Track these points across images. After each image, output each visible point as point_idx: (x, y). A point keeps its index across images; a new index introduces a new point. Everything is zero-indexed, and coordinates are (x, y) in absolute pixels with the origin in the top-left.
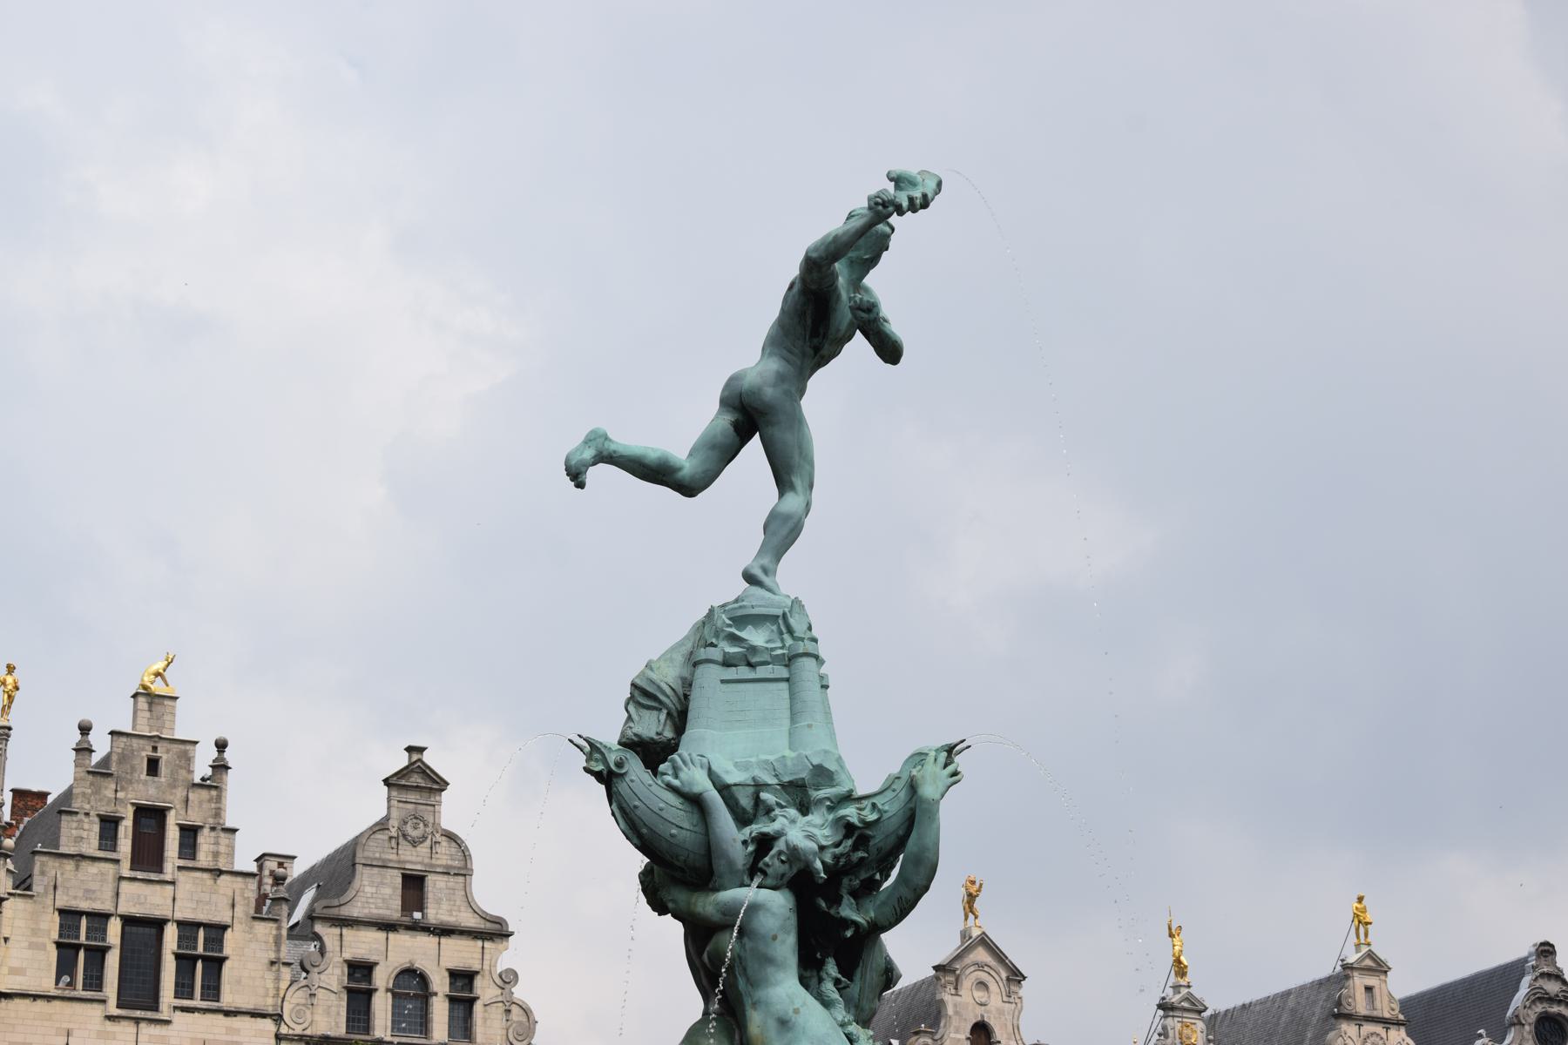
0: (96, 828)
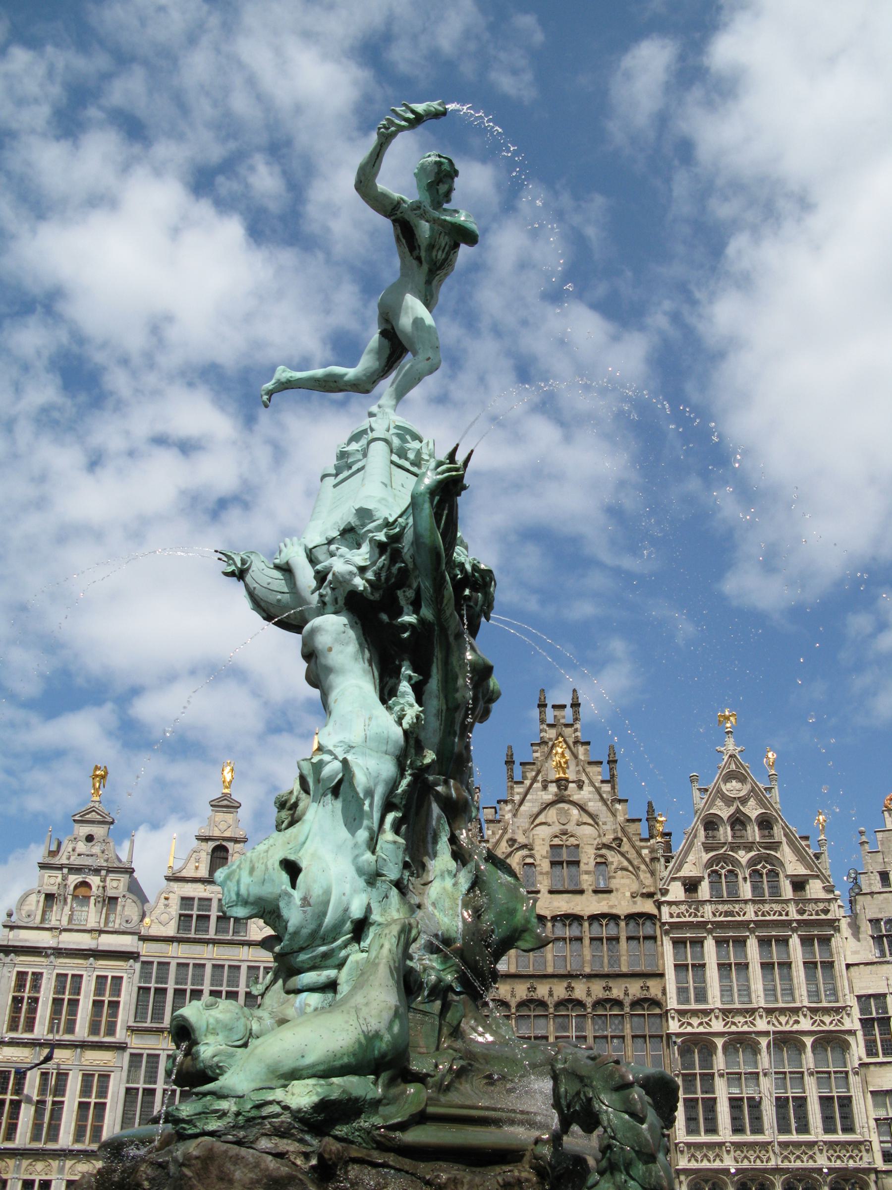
0: (878, 878)
